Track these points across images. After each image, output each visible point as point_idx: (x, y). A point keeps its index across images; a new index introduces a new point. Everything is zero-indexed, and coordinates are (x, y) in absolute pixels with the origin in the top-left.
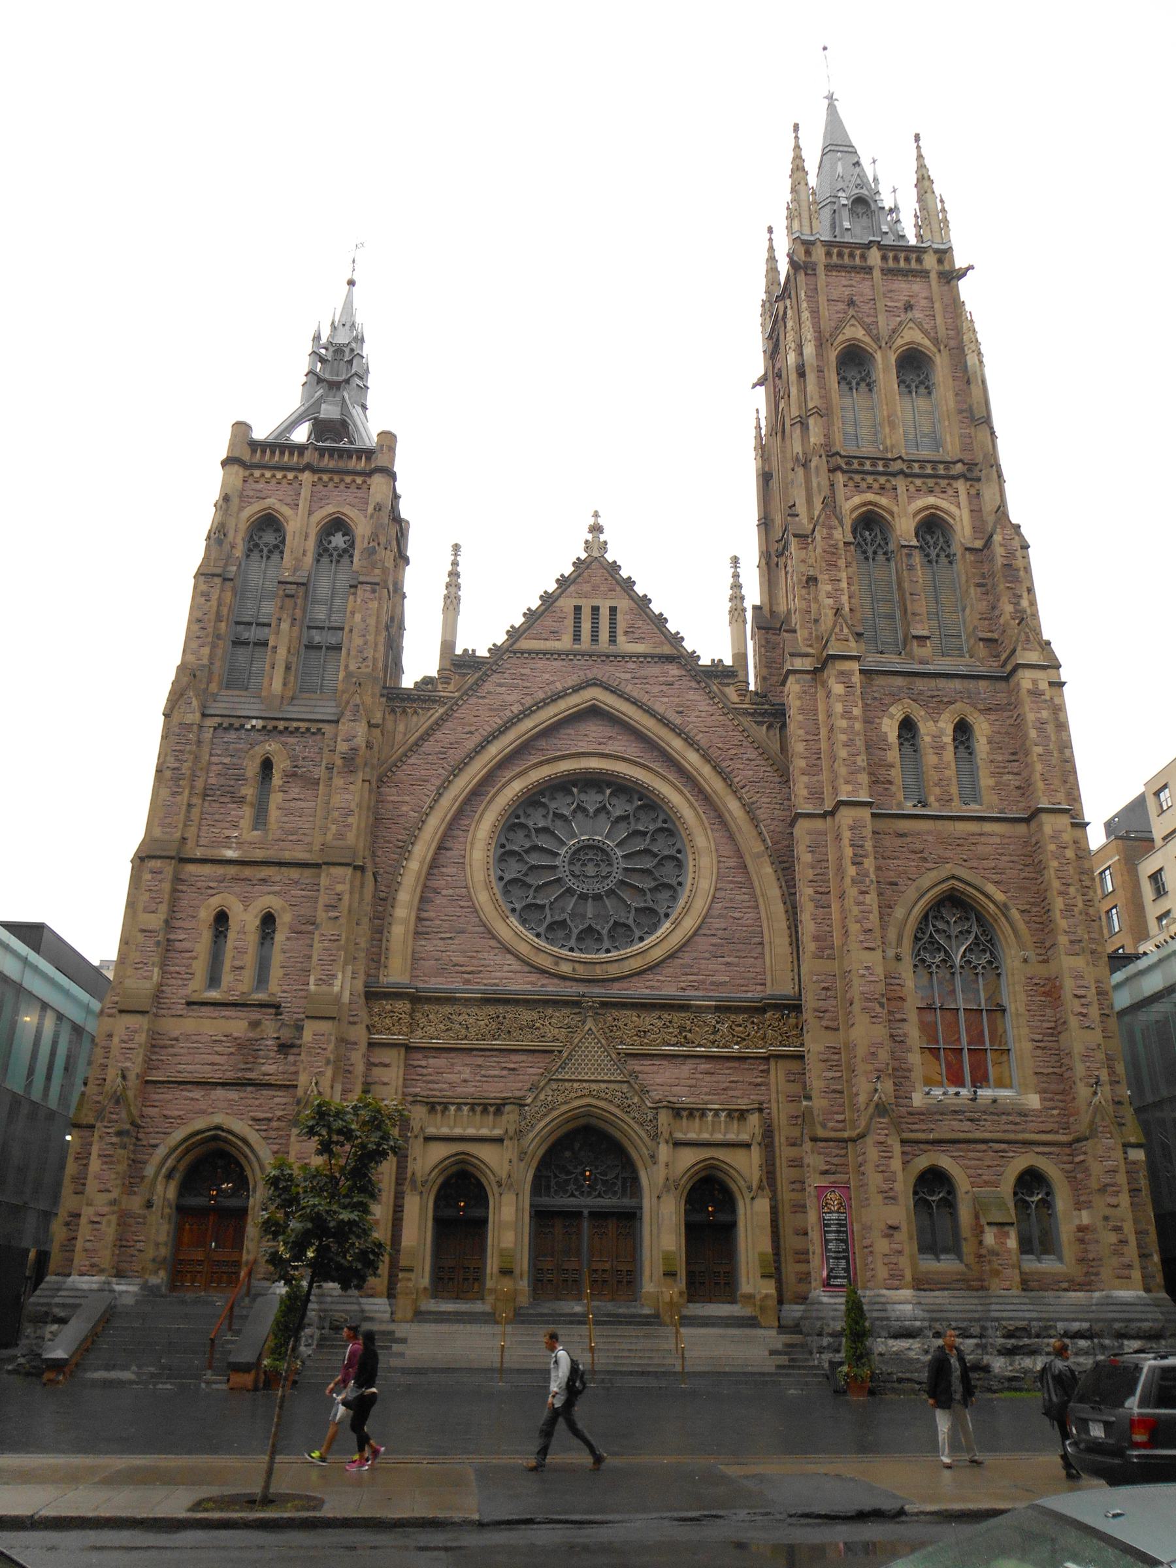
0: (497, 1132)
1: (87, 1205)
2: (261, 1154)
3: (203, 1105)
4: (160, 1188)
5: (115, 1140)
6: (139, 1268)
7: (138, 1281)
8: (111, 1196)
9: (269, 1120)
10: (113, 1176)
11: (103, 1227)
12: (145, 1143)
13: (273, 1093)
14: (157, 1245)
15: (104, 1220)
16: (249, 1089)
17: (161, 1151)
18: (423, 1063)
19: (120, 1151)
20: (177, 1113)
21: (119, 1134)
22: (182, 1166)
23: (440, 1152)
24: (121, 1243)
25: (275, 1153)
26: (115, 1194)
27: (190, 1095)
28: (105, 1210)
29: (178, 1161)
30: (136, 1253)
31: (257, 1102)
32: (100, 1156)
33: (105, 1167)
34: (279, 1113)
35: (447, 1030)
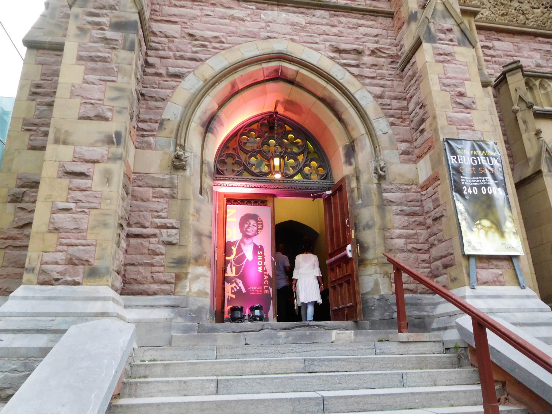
1: (57, 141)
2: (358, 96)
3: (250, 26)
6: (169, 276)
8: (111, 128)
9: (359, 53)
10: (115, 94)
11: (95, 183)
12: (163, 71)
13: (355, 21)
15: (97, 171)
16: (319, 13)
17: (191, 84)
18: (490, 45)
24: (132, 231)
25: (381, 97)
26: (119, 123)
28: (100, 151)
30: (162, 248)
31: (335, 30)
32: (80, 58)
33: (92, 77)
34: (373, 46)
35: (503, 15)
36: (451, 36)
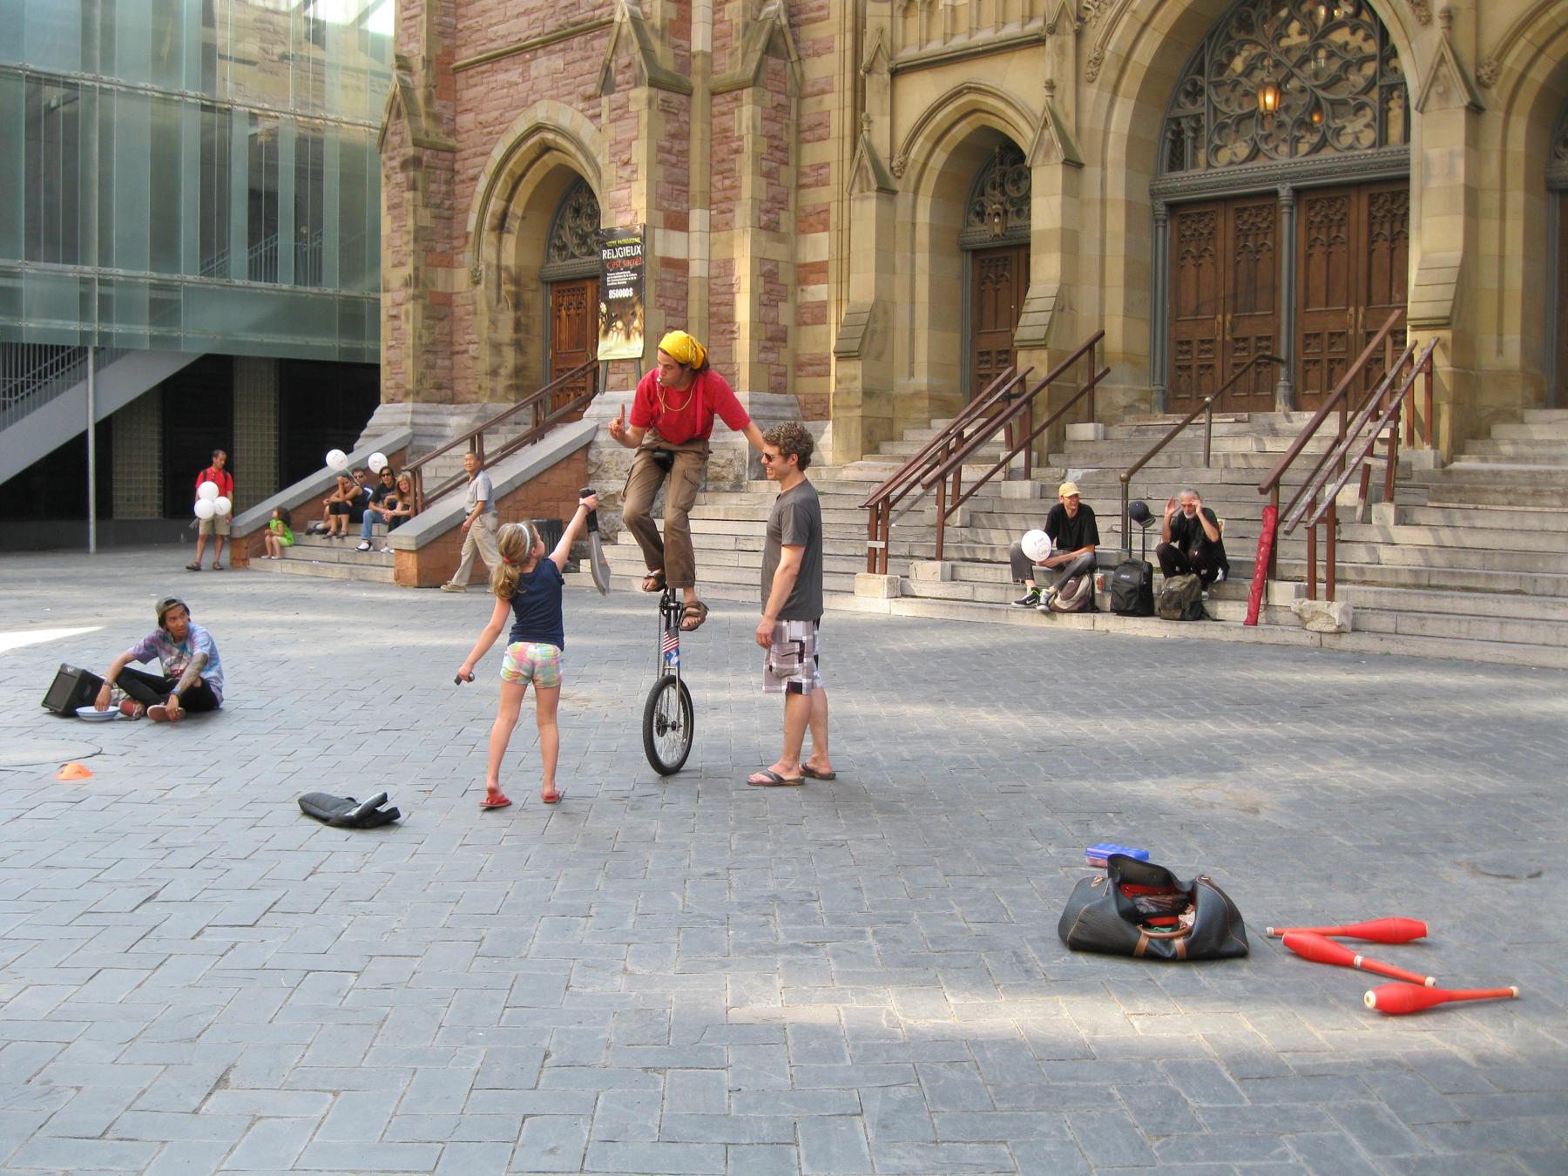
0: (1035, 26)
4: (488, 253)
5: (400, 177)
7: (475, 407)
12: (463, 177)
14: (496, 347)
16: (576, 42)
17: (482, 185)
19: (409, 195)
20: (496, 114)
21: (404, 166)
22: (517, 208)
23: (921, 93)
27: (502, 77)
29: (509, 199)
30: (470, 363)
36: (629, 74)
